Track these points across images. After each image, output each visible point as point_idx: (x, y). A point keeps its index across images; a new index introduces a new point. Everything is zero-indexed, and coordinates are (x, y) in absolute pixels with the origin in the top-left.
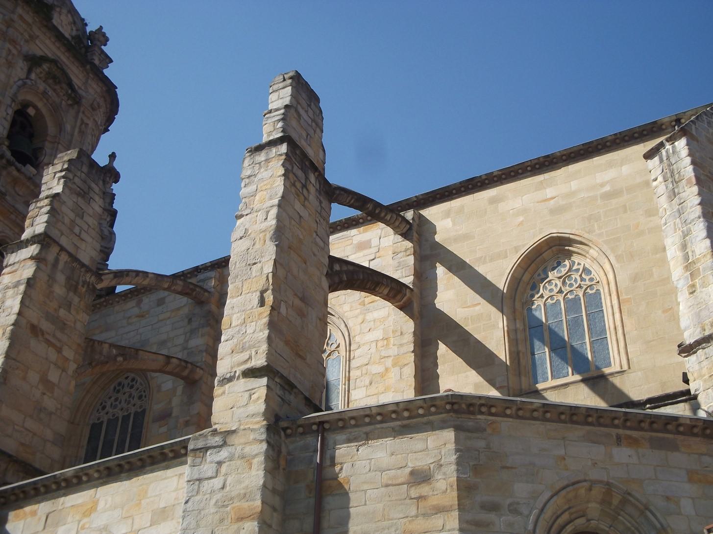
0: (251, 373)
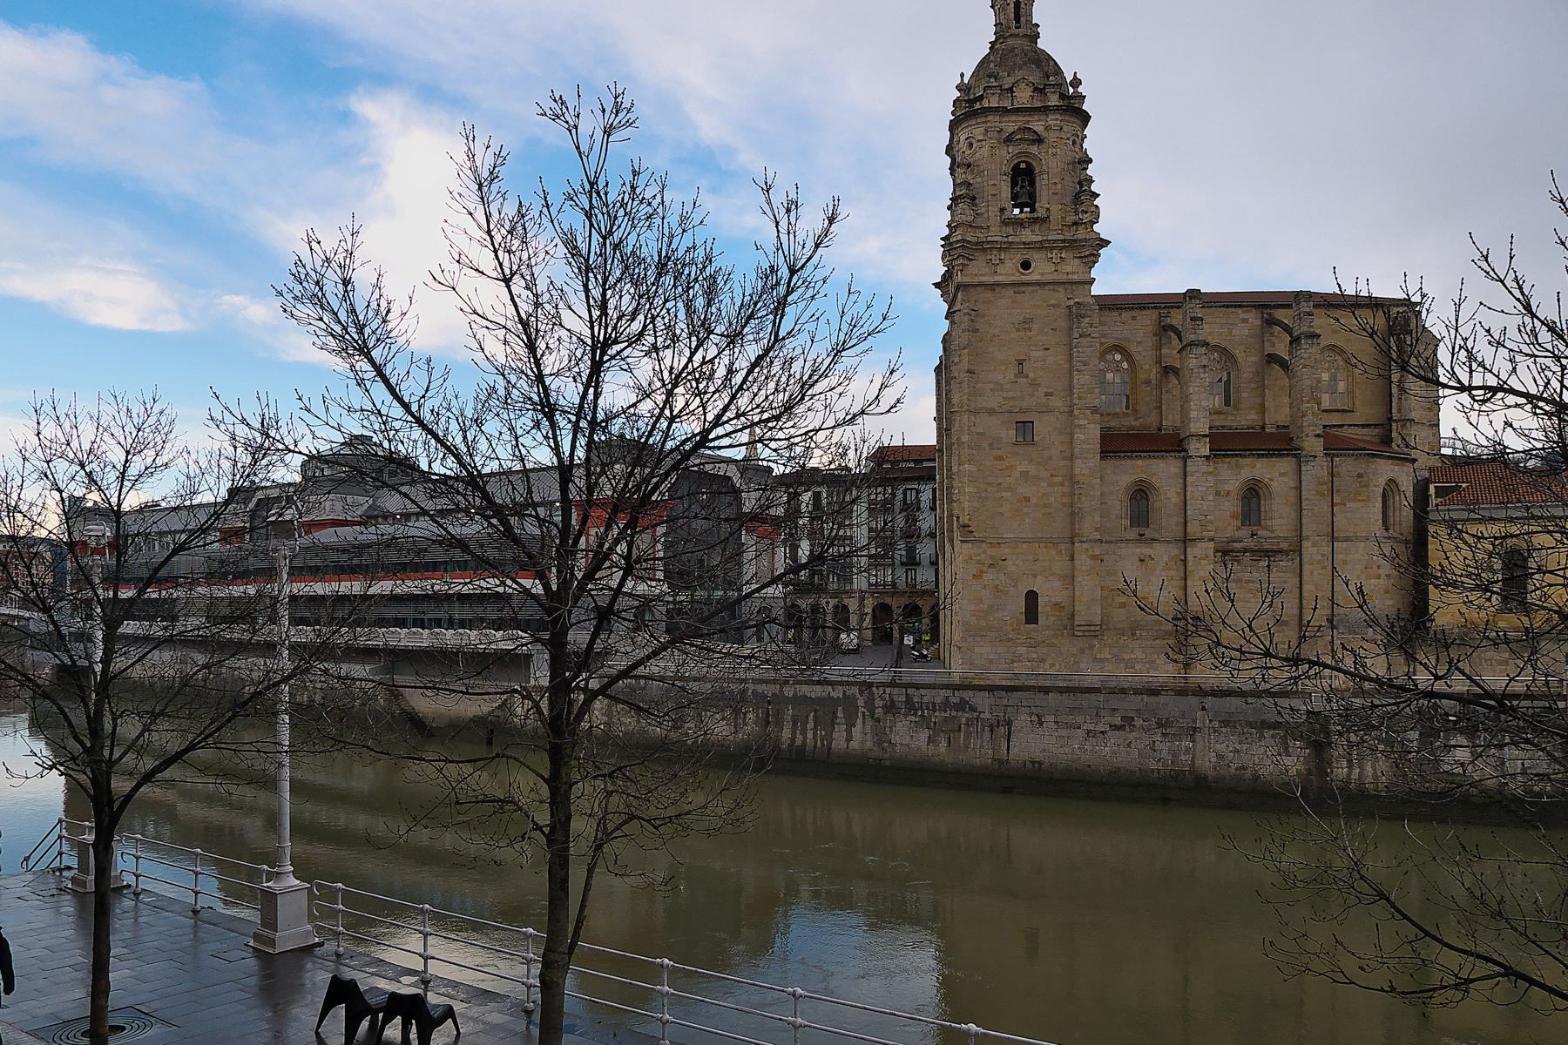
0: (1318, 436)
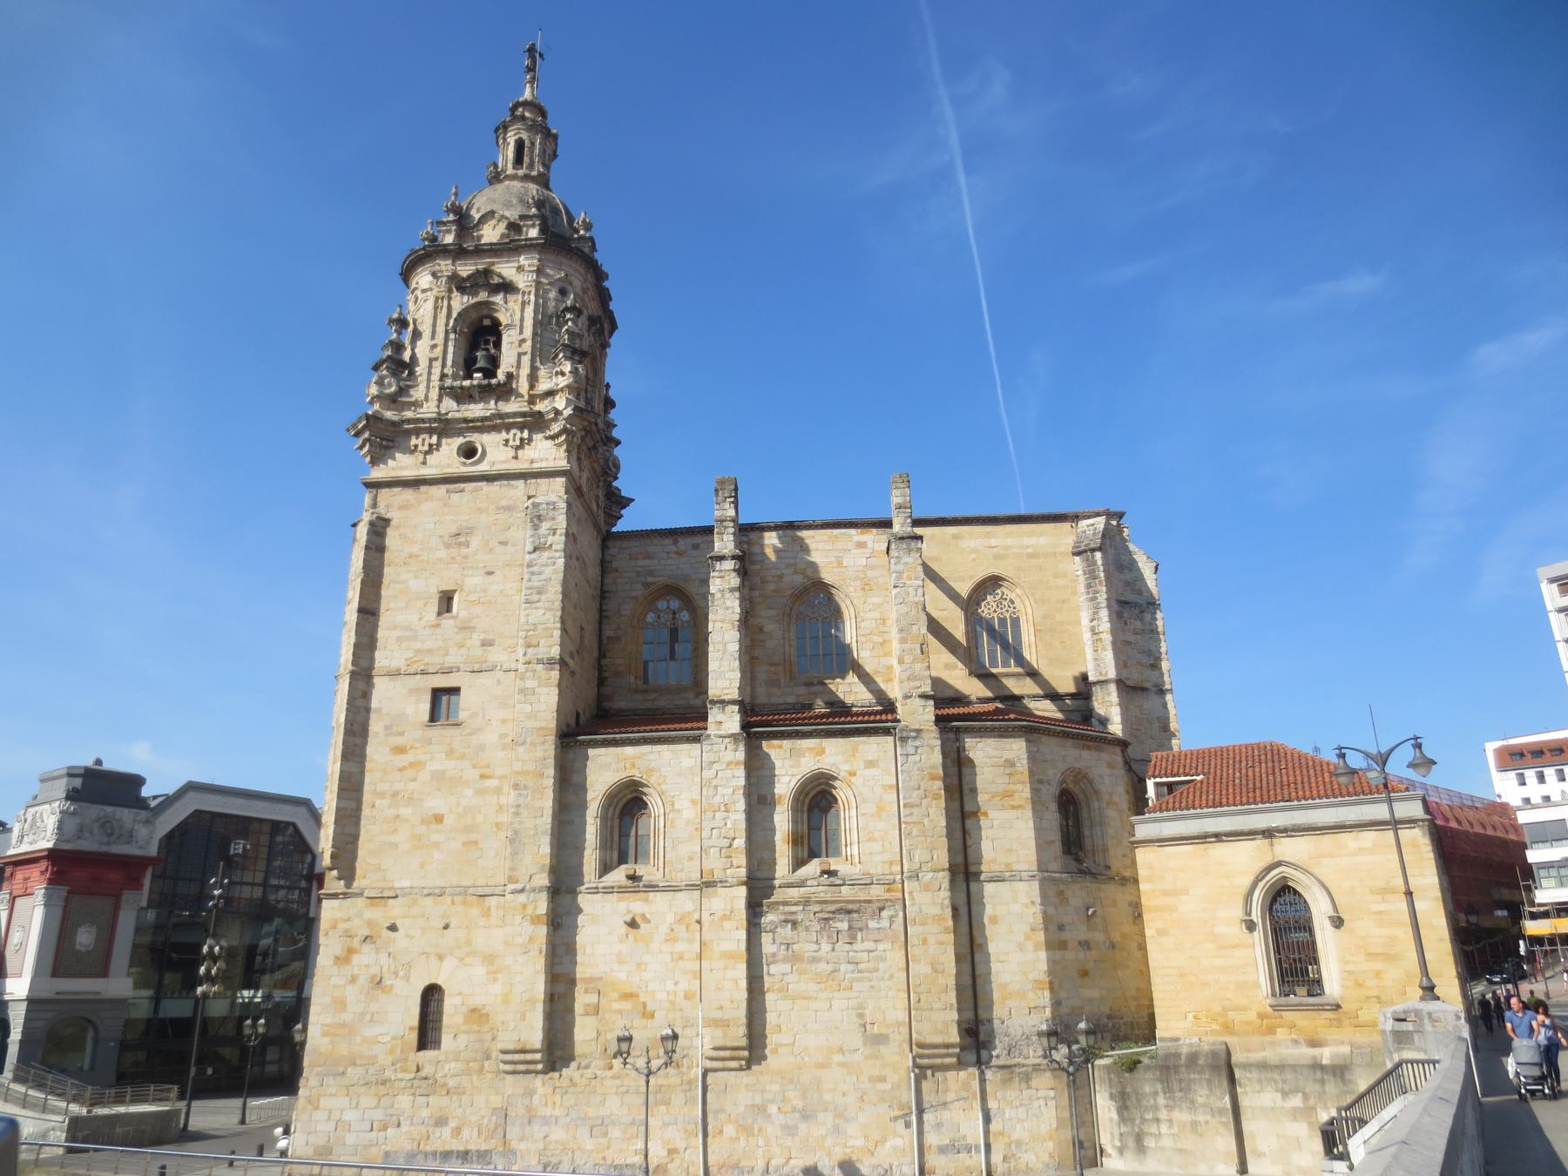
0: (924, 696)
